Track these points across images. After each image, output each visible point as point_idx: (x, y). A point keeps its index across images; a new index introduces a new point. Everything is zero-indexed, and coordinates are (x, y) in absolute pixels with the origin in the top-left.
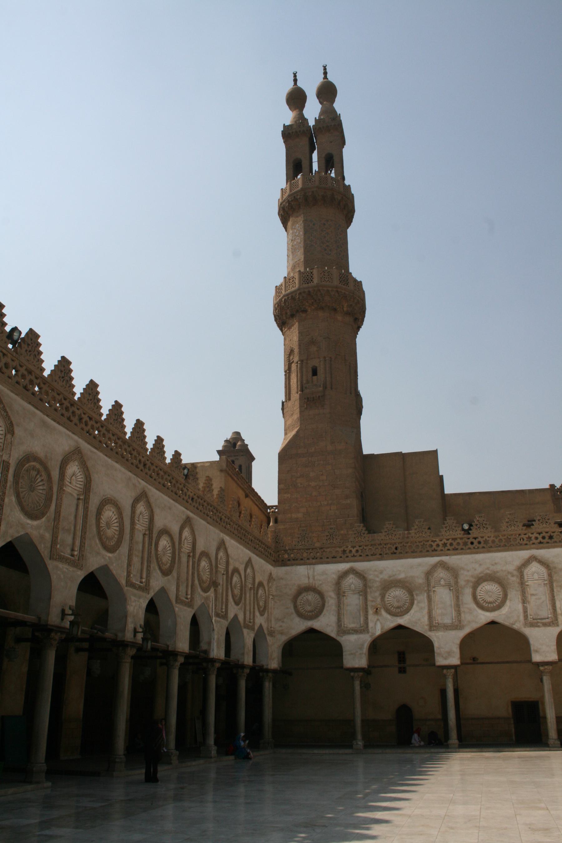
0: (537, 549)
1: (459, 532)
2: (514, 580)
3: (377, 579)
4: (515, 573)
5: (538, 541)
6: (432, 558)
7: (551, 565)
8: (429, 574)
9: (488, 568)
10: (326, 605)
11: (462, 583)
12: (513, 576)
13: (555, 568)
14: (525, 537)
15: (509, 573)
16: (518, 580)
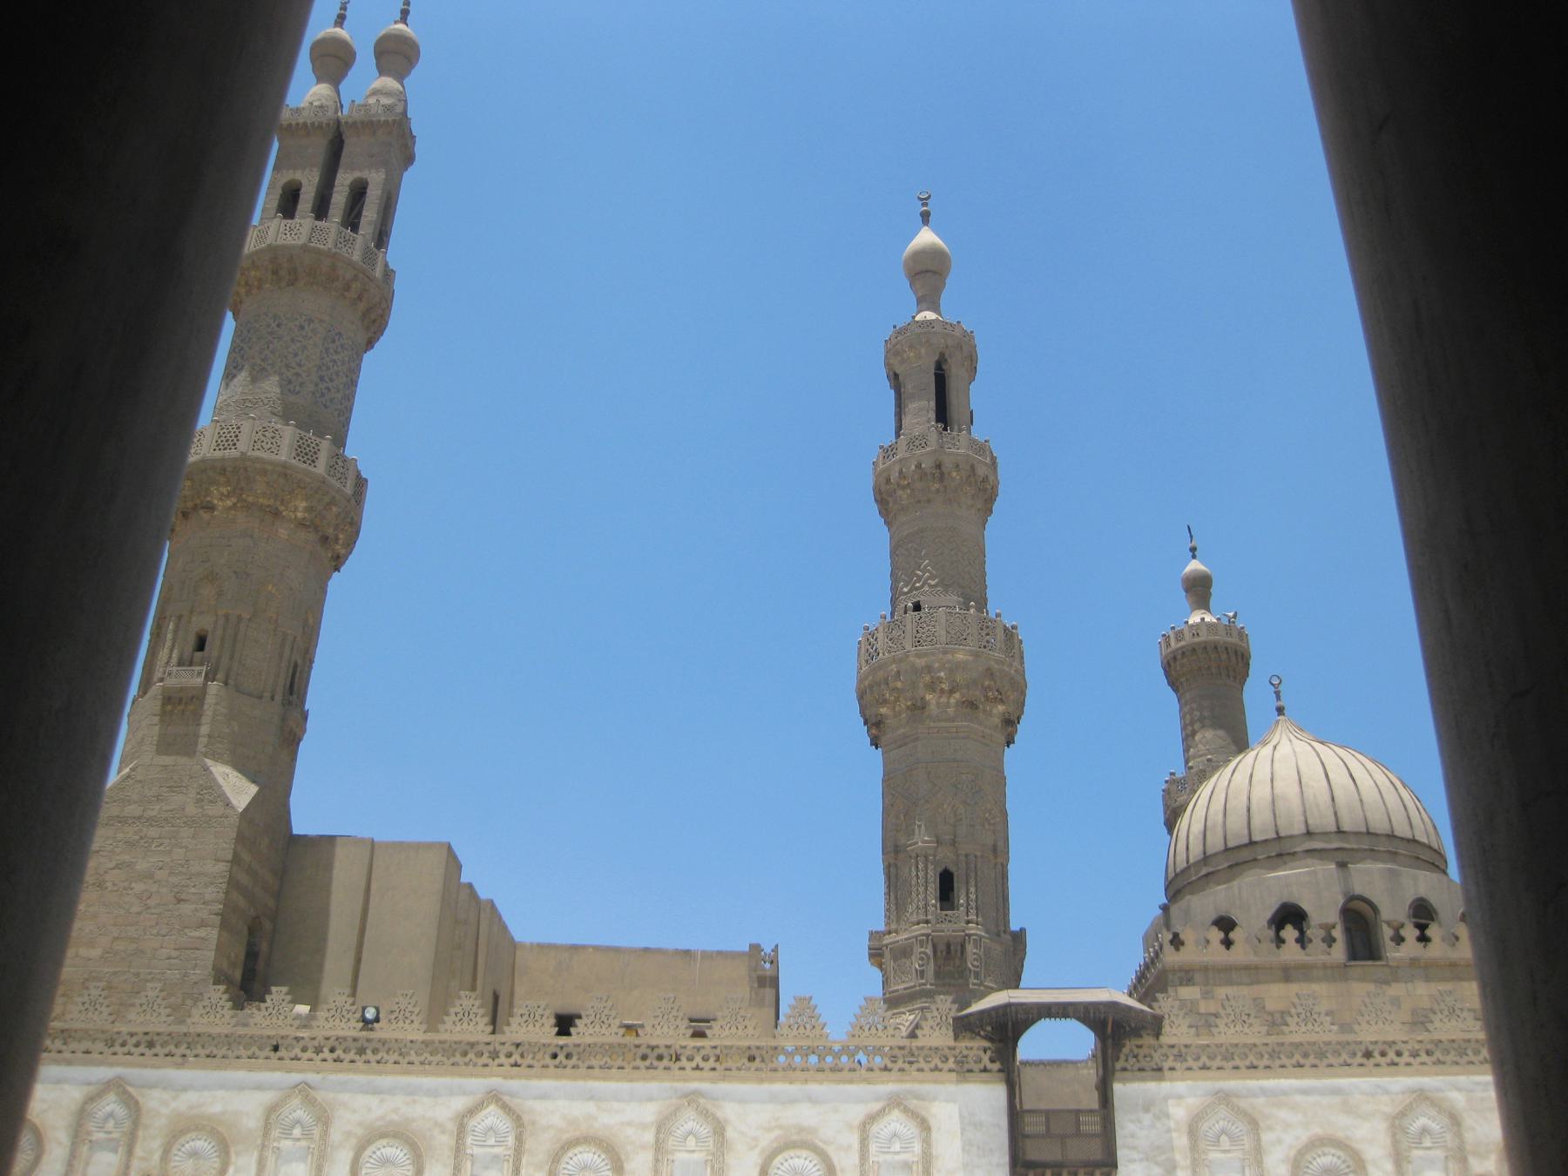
0: (505, 1077)
1: (353, 1023)
2: (445, 1141)
3: (165, 1111)
4: (451, 1127)
5: (512, 1060)
6: (287, 1076)
7: (525, 1118)
8: (272, 1110)
9: (396, 1111)
10: (45, 1159)
11: (336, 1135)
12: (443, 1132)
13: (533, 1123)
14: (486, 1049)
15: (436, 1124)
16: (453, 1143)
